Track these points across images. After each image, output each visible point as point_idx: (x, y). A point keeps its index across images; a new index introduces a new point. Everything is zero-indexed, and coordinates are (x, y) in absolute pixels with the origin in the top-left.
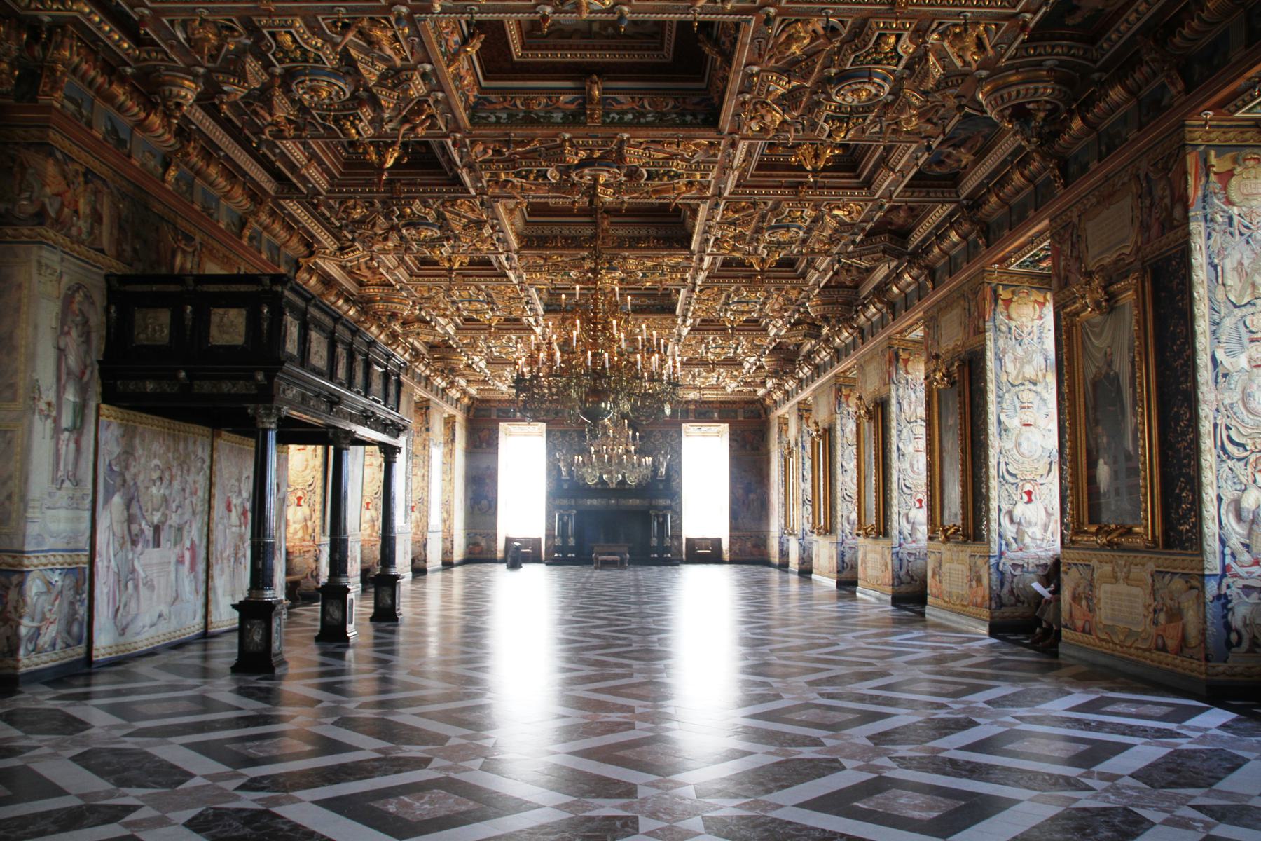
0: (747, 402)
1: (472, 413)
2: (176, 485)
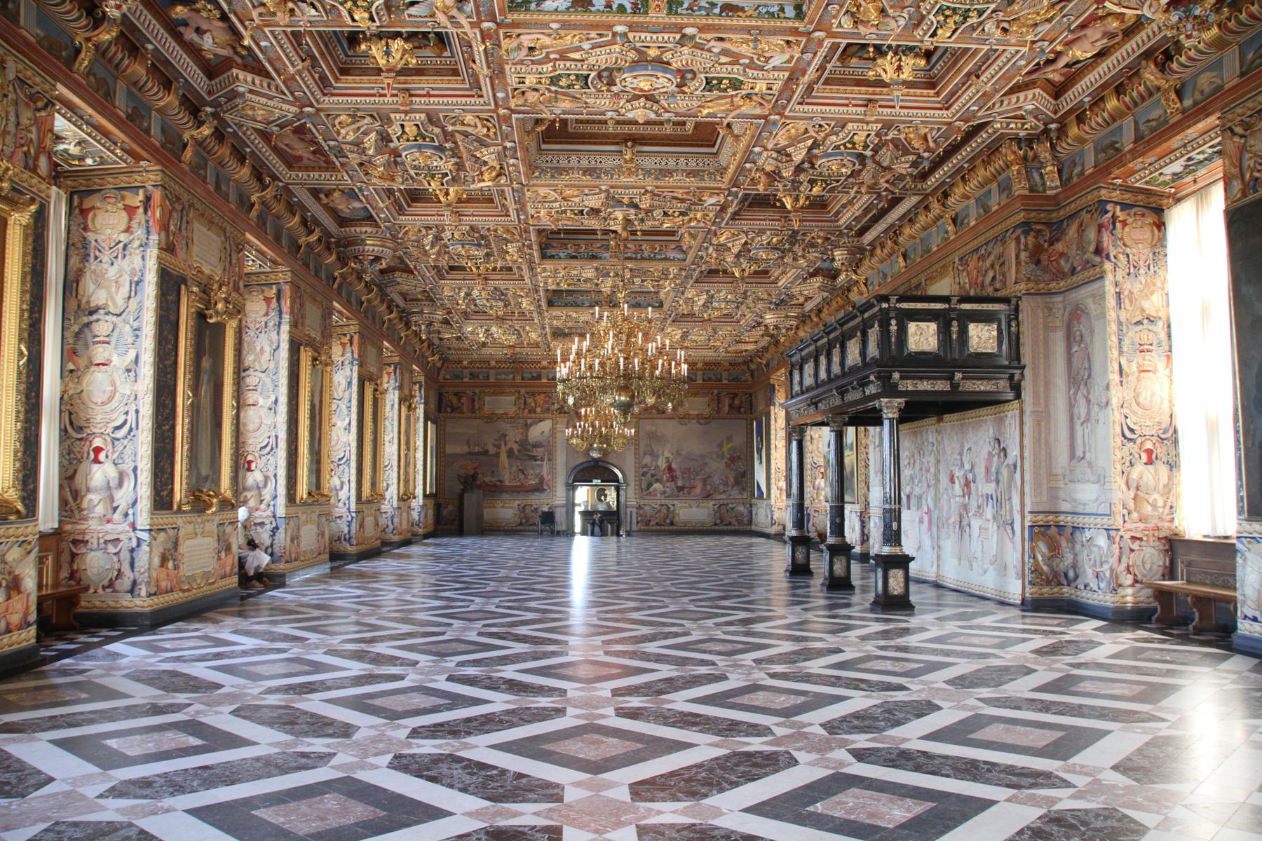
2: (917, 466)
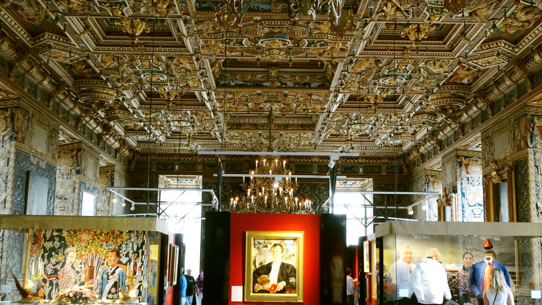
0: (390, 158)
1: (132, 167)
